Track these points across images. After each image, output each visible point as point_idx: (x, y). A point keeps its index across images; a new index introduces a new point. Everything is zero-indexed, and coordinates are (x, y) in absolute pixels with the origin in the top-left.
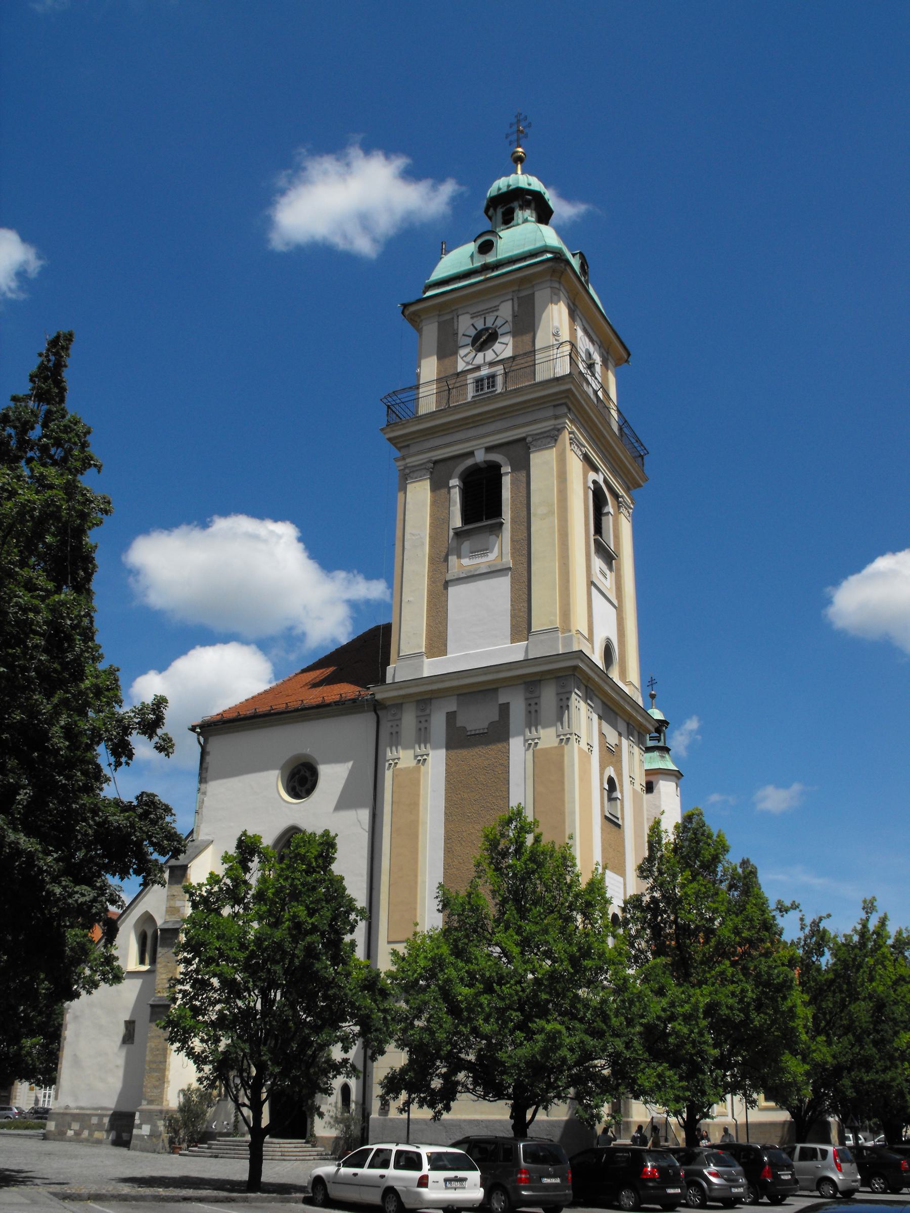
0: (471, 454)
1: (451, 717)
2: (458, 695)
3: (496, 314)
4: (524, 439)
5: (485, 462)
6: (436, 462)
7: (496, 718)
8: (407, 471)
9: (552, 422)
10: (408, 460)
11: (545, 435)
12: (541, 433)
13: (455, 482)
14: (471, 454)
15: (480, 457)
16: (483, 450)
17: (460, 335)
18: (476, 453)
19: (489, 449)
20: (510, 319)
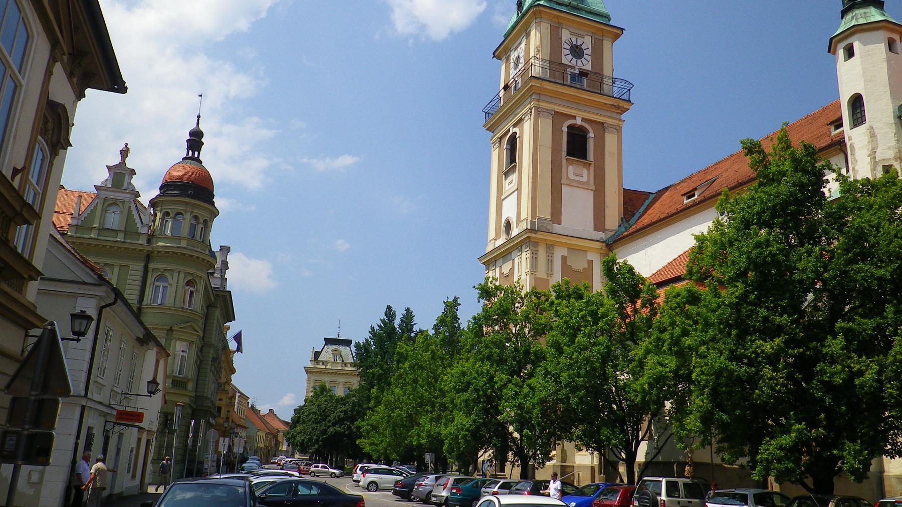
0: (574, 117)
1: (564, 259)
2: (568, 248)
3: (582, 39)
4: (603, 123)
5: (581, 125)
6: (556, 112)
7: (586, 267)
8: (540, 110)
9: (617, 122)
10: (540, 103)
11: (612, 126)
12: (611, 125)
13: (565, 129)
14: (574, 117)
15: (579, 122)
16: (581, 118)
17: (563, 41)
18: (577, 118)
19: (583, 119)
20: (590, 47)
